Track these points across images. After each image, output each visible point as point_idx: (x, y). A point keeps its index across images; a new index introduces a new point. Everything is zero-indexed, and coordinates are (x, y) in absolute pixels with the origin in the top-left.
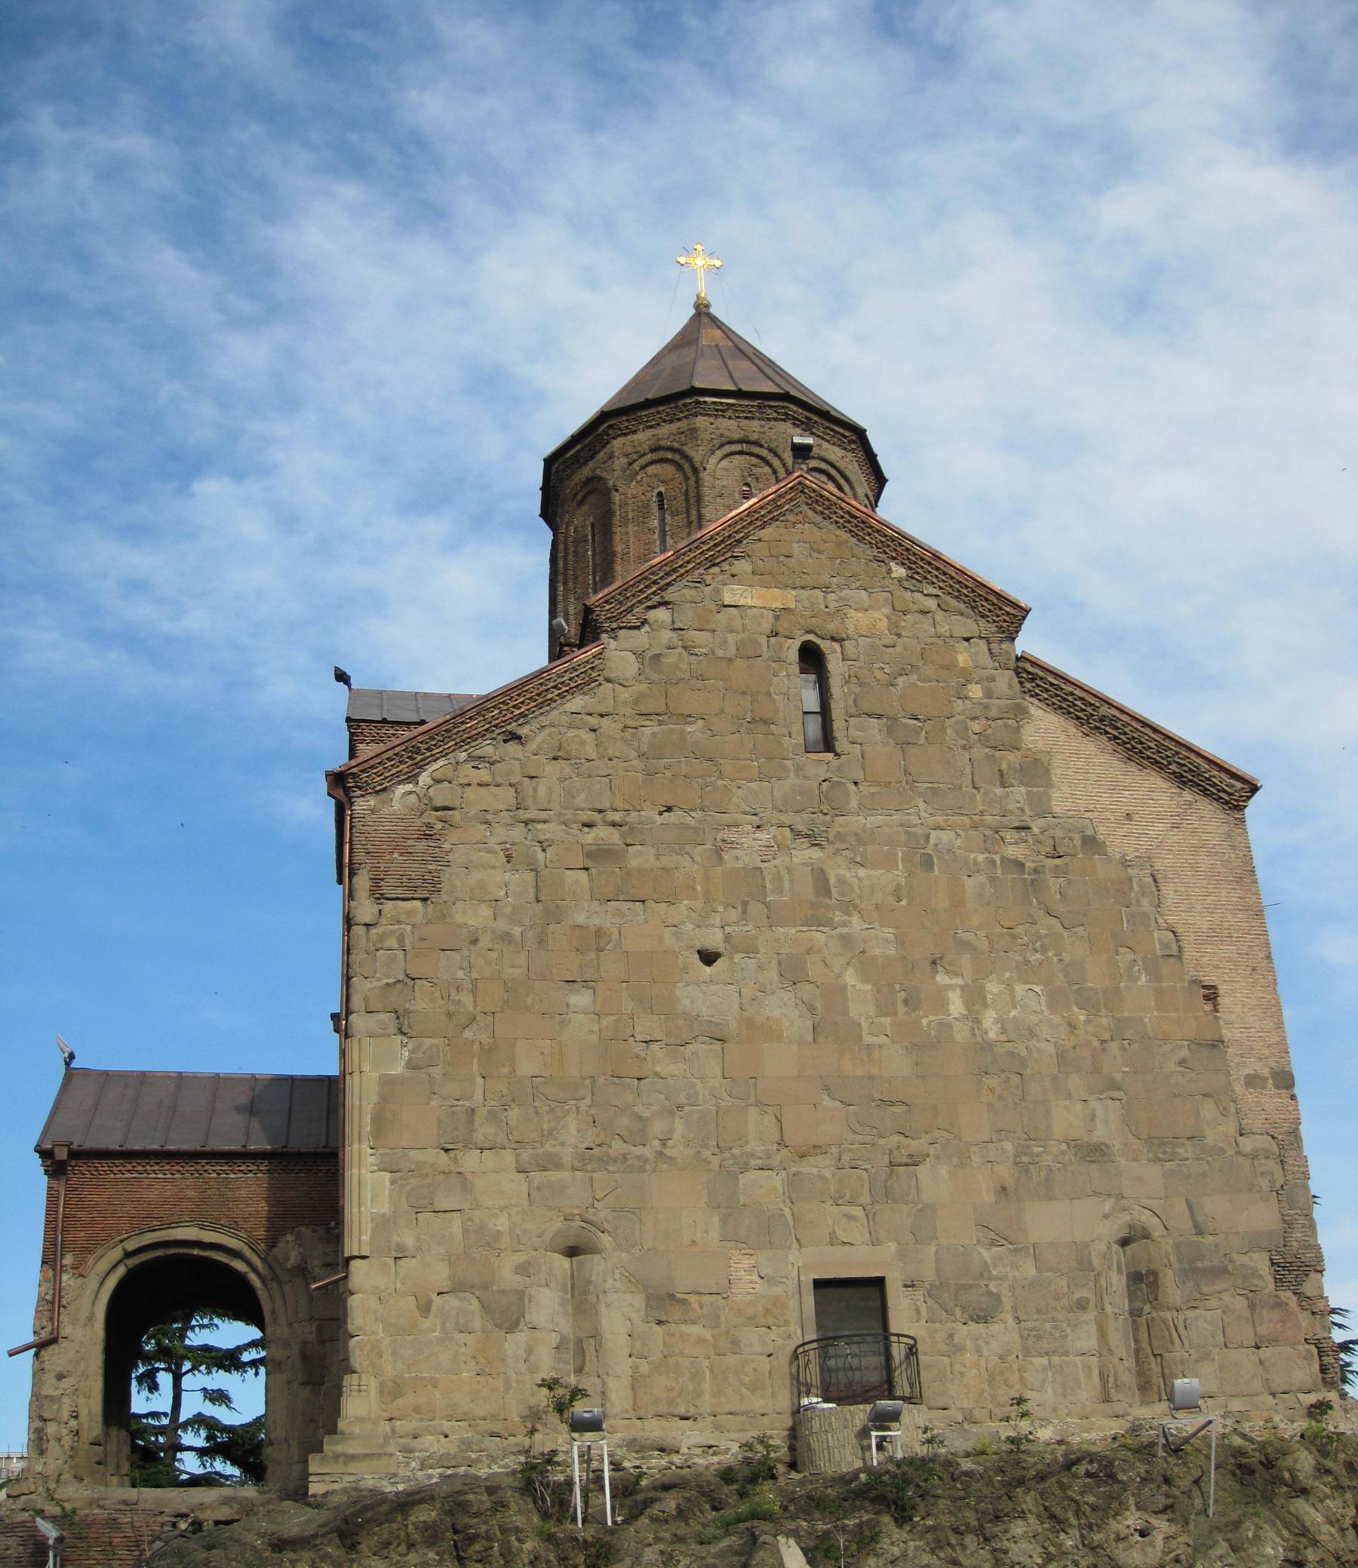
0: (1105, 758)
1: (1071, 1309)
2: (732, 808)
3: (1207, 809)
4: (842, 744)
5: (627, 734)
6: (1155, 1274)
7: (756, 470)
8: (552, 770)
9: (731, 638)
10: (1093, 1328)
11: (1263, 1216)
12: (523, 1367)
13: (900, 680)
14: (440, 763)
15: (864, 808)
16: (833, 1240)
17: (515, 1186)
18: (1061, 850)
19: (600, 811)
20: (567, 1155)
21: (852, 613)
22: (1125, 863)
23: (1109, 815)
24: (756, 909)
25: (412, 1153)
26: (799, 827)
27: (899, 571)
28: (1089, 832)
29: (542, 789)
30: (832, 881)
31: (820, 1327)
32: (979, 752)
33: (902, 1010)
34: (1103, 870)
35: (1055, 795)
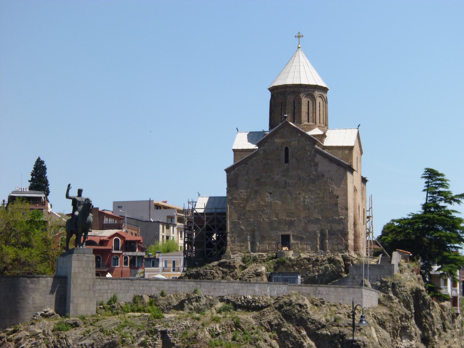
27: (299, 135)
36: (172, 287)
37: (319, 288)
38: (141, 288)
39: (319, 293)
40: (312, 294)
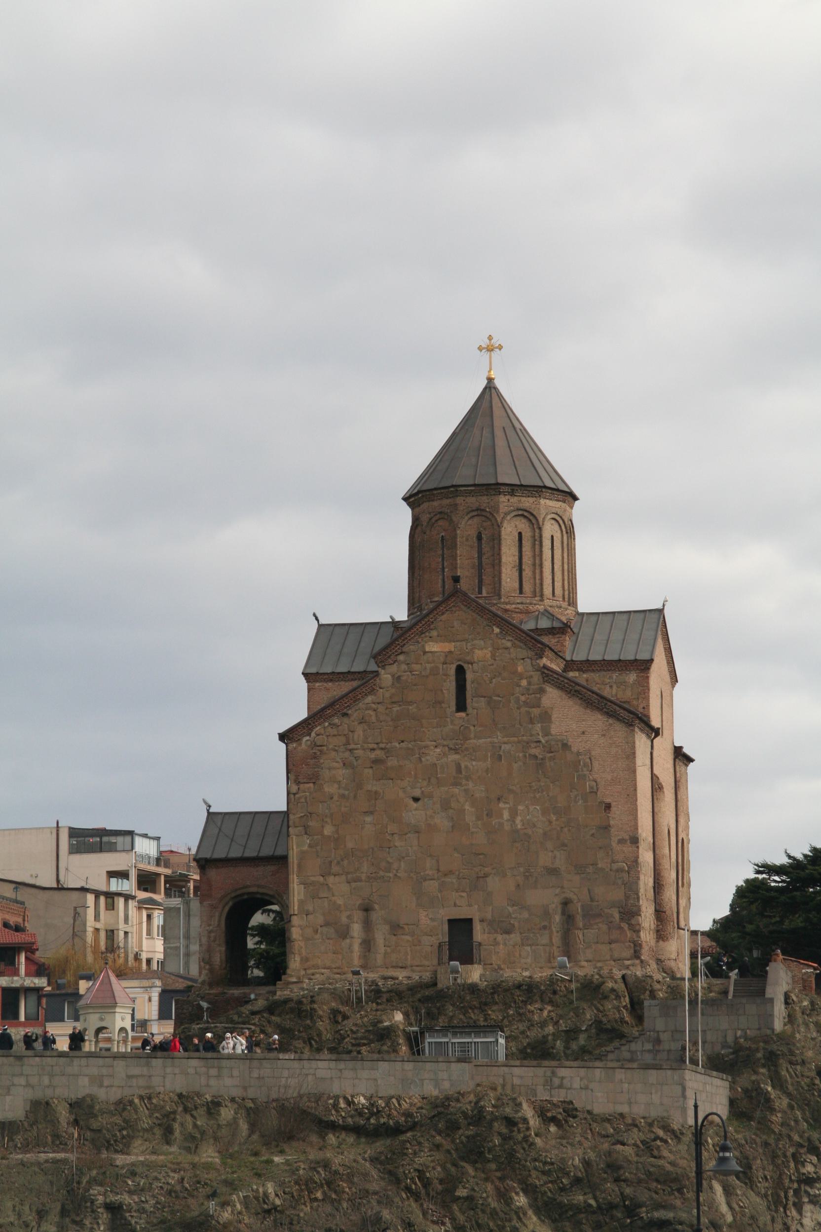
3: (618, 726)
4: (470, 710)
5: (387, 711)
7: (485, 524)
9: (428, 666)
11: (617, 894)
17: (345, 888)
20: (363, 876)
21: (476, 651)
22: (578, 754)
26: (451, 746)
27: (497, 630)
29: (356, 737)
30: (463, 767)
32: (524, 710)
35: (553, 726)
36: (137, 1076)
37: (562, 1072)
38: (46, 1080)
39: (561, 1086)
40: (540, 1088)
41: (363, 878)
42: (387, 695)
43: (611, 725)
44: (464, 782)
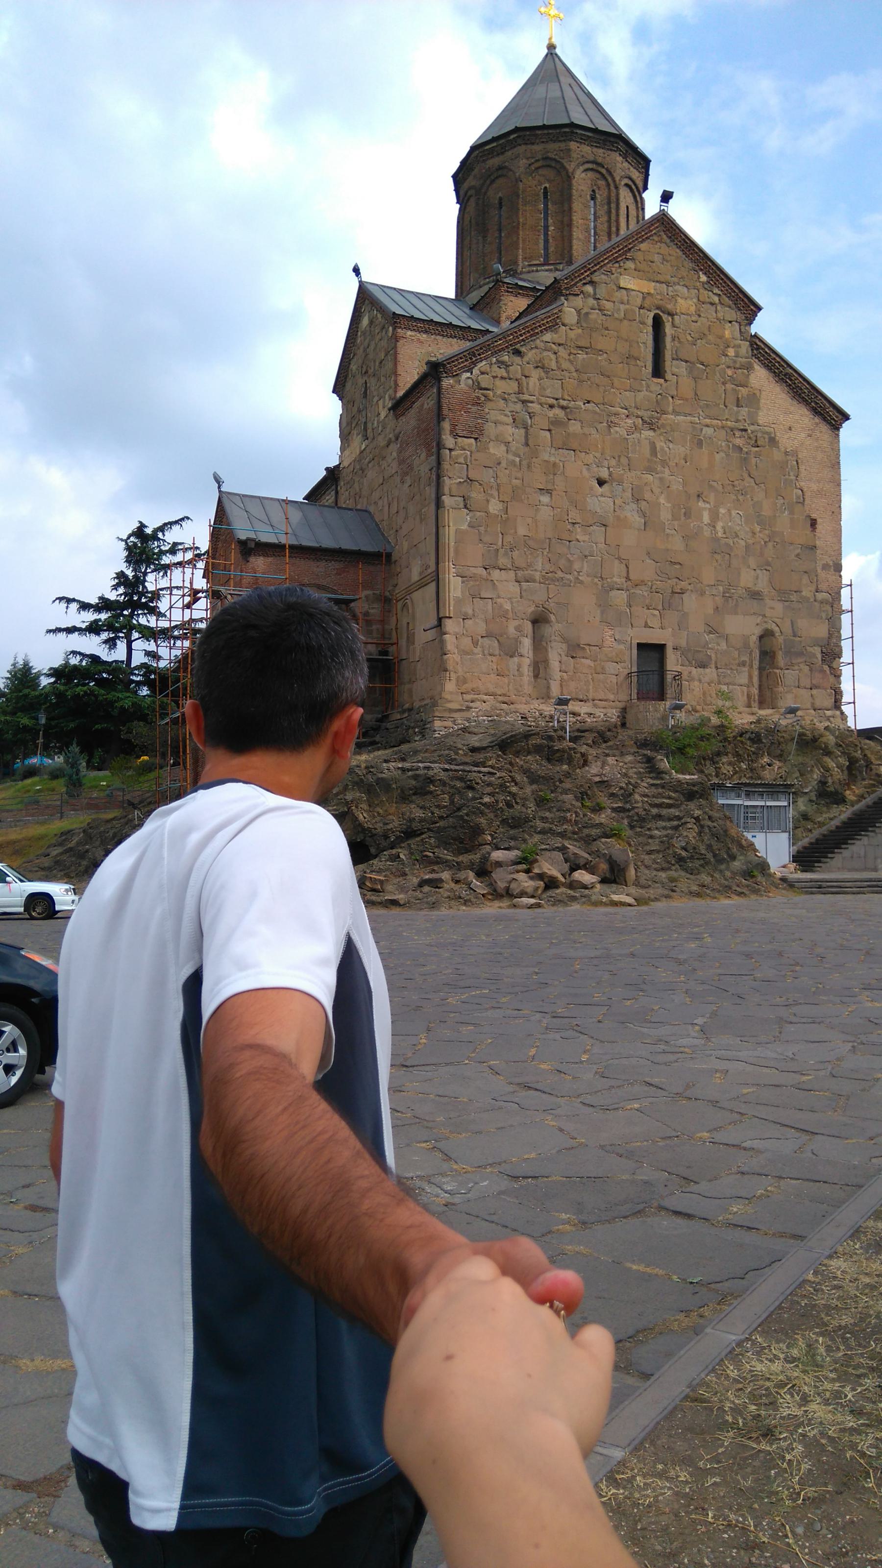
0: (784, 396)
1: (739, 665)
2: (617, 405)
3: (824, 427)
4: (668, 376)
6: (774, 653)
8: (535, 374)
9: (622, 307)
10: (746, 674)
11: (821, 631)
12: (516, 673)
13: (699, 341)
14: (484, 363)
15: (676, 413)
16: (646, 626)
17: (514, 588)
18: (759, 443)
19: (557, 399)
22: (786, 453)
23: (781, 427)
24: (624, 461)
25: (471, 569)
27: (704, 278)
28: (773, 435)
29: (531, 384)
30: (658, 449)
31: (638, 665)
32: (729, 386)
33: (683, 518)
34: (777, 455)
41: (537, 578)
42: (572, 334)
43: (817, 424)
44: (659, 468)
